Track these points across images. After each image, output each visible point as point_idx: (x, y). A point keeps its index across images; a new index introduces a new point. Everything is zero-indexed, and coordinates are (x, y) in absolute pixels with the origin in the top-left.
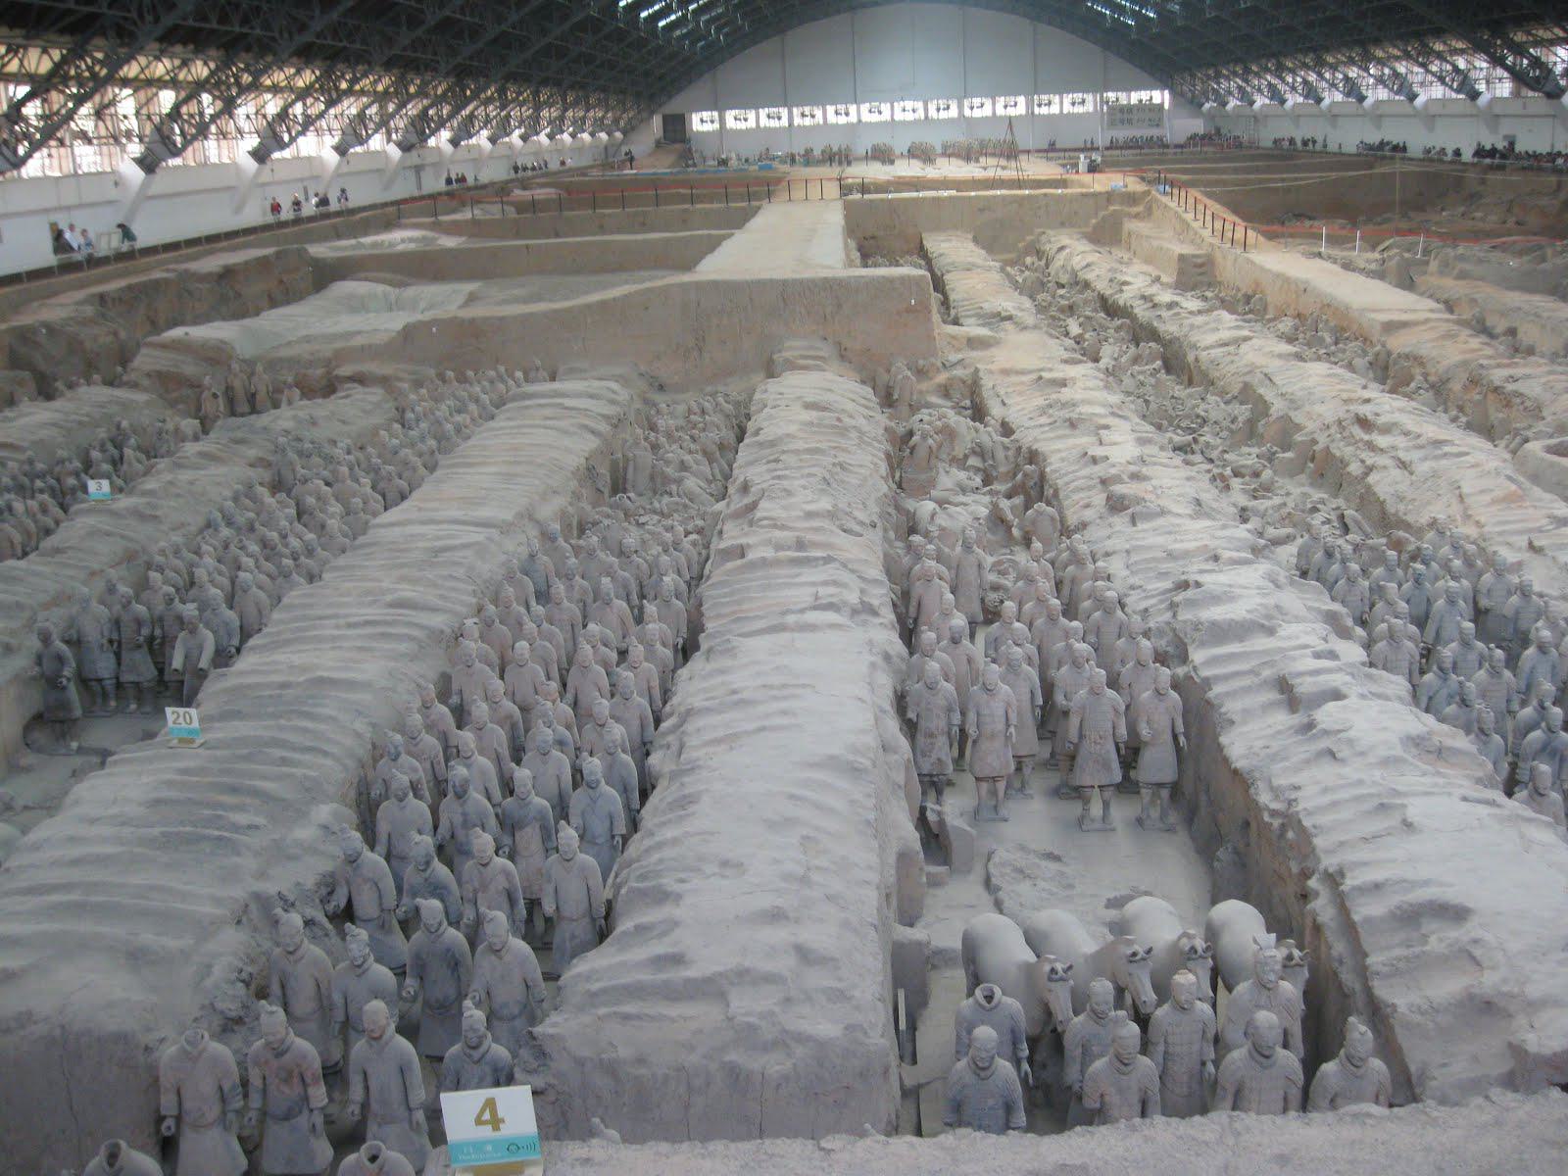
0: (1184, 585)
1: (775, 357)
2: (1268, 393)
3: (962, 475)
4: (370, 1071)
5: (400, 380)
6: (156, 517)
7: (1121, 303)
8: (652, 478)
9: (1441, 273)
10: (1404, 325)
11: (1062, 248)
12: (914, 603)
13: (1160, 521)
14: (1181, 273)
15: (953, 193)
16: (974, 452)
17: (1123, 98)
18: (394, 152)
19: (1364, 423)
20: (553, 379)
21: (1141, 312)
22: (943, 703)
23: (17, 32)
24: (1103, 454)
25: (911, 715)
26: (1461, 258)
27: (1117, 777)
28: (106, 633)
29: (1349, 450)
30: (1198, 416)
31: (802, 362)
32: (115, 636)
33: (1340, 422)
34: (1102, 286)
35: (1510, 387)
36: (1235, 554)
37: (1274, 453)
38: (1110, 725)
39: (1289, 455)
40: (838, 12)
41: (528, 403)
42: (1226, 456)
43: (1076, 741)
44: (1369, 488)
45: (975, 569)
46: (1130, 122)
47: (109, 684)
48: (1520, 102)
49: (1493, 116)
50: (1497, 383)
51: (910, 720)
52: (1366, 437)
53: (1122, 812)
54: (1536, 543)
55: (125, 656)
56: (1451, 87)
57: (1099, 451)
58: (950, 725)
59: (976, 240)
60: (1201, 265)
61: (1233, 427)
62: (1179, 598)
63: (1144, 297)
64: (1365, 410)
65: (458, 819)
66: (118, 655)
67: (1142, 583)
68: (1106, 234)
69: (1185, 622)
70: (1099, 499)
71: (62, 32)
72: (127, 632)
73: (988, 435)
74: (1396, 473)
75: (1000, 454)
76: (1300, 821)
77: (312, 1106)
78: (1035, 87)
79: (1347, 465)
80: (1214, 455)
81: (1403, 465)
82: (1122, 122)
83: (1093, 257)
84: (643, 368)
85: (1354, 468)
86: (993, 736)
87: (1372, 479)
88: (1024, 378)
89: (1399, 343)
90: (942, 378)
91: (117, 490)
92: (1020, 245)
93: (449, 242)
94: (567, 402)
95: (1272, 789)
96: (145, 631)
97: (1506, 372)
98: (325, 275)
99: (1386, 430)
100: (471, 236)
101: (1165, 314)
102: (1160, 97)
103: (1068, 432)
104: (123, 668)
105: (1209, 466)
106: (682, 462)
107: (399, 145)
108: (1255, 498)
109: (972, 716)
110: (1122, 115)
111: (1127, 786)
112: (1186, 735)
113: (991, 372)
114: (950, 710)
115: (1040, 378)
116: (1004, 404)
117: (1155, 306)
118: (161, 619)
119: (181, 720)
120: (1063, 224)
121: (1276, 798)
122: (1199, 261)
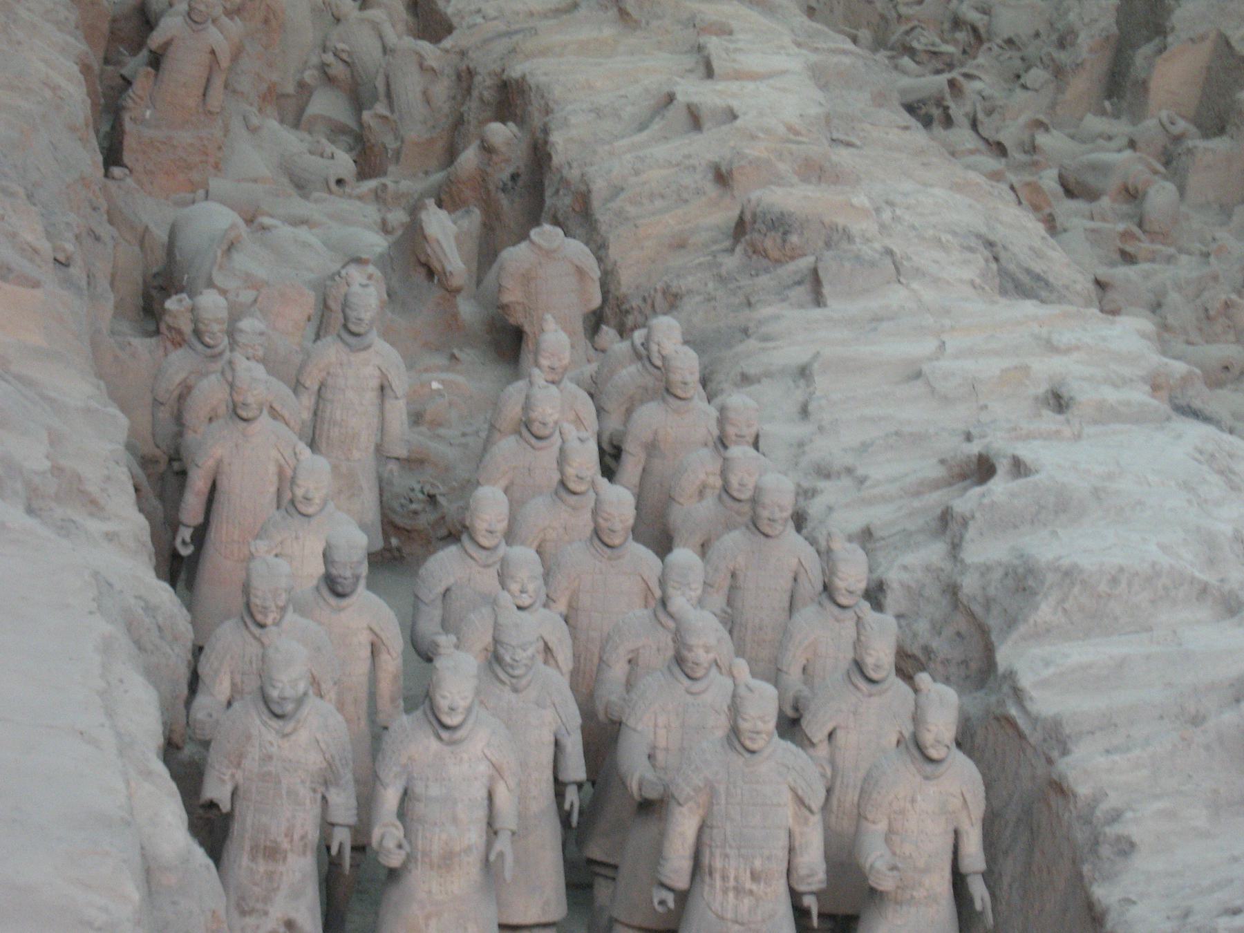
3: (293, 142)
12: (198, 483)
13: (896, 297)
16: (329, 79)
22: (314, 761)
24: (720, 102)
25: (216, 790)
30: (957, 23)
36: (1111, 395)
37: (1178, 139)
38: (783, 842)
39: (1220, 144)
42: (1042, 139)
43: (682, 883)
45: (371, 396)
51: (212, 805)
57: (692, 90)
58: (327, 826)
61: (1062, 57)
62: (968, 500)
67: (849, 460)
69: (985, 570)
75: (410, 86)
80: (1008, 136)
86: (448, 860)
103: (608, 32)
105: (993, 163)
108: (1128, 258)
109: (390, 798)
112: (990, 877)
114: (327, 779)
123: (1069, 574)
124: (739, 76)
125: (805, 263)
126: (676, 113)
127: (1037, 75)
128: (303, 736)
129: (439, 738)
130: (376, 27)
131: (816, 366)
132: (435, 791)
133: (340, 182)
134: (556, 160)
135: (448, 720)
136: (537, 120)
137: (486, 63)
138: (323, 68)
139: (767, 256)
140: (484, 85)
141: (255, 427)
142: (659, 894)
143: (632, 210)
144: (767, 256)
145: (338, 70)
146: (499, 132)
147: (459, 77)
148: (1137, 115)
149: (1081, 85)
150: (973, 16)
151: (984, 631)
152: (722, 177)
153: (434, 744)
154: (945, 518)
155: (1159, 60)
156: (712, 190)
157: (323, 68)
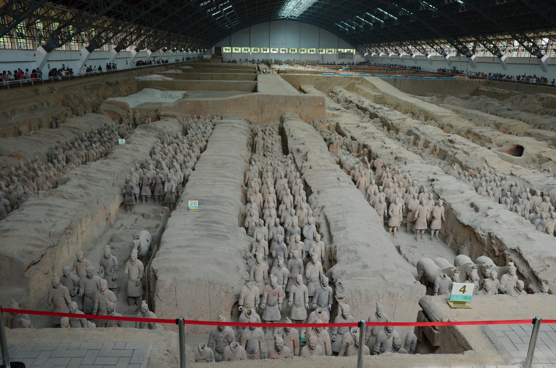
0: (433, 180)
3: (343, 151)
4: (296, 293)
5: (178, 117)
6: (138, 150)
7: (364, 107)
8: (263, 147)
9: (448, 104)
10: (445, 116)
11: (340, 91)
12: (358, 182)
14: (375, 99)
15: (309, 74)
17: (342, 50)
18: (149, 52)
19: (451, 141)
20: (222, 119)
21: (370, 109)
22: (384, 207)
23: (65, 6)
26: (453, 99)
27: (426, 228)
28: (138, 181)
29: (447, 148)
30: (397, 138)
32: (141, 182)
33: (443, 141)
34: (356, 102)
35: (481, 134)
40: (266, 21)
41: (223, 125)
44: (456, 158)
46: (344, 57)
47: (137, 196)
48: (458, 58)
49: (450, 61)
50: (477, 133)
52: (452, 145)
53: (425, 237)
54: (514, 173)
55: (144, 188)
56: (439, 53)
58: (385, 213)
59: (315, 87)
60: (380, 98)
62: (433, 183)
63: (371, 106)
64: (450, 138)
65: (275, 232)
66: (141, 188)
68: (351, 88)
69: (437, 189)
70: (392, 157)
71: (76, 8)
72: (145, 181)
73: (348, 140)
74: (465, 155)
75: (354, 145)
76: (496, 237)
77: (279, 302)
78: (319, 46)
79: (447, 152)
81: (465, 153)
82: (342, 57)
83: (351, 94)
84: (246, 118)
85: (450, 153)
87: (457, 156)
88: (353, 126)
89: (445, 121)
90: (327, 124)
91: (127, 143)
92: (327, 90)
93: (167, 79)
94: (235, 125)
95: (481, 229)
96: (150, 181)
97: (480, 130)
98: (142, 86)
99: (459, 143)
100: (175, 78)
101: (379, 111)
102: (353, 51)
104: (142, 191)
106: (272, 143)
107: (151, 50)
110: (342, 55)
111: (428, 231)
113: (342, 123)
115: (359, 126)
116: (349, 132)
117: (374, 108)
118: (155, 178)
119: (193, 204)
120: (339, 85)
121: (484, 232)
122: (380, 97)
123: (446, 190)
125: (404, 161)
126: (384, 148)
127: (406, 143)
137: (362, 143)
138: (344, 144)
140: (362, 145)
142: (414, 219)
145: (345, 144)
146: (365, 149)
148: (417, 146)
149: (411, 144)
151: (438, 195)
152: (392, 153)
154: (431, 185)
157: (344, 144)
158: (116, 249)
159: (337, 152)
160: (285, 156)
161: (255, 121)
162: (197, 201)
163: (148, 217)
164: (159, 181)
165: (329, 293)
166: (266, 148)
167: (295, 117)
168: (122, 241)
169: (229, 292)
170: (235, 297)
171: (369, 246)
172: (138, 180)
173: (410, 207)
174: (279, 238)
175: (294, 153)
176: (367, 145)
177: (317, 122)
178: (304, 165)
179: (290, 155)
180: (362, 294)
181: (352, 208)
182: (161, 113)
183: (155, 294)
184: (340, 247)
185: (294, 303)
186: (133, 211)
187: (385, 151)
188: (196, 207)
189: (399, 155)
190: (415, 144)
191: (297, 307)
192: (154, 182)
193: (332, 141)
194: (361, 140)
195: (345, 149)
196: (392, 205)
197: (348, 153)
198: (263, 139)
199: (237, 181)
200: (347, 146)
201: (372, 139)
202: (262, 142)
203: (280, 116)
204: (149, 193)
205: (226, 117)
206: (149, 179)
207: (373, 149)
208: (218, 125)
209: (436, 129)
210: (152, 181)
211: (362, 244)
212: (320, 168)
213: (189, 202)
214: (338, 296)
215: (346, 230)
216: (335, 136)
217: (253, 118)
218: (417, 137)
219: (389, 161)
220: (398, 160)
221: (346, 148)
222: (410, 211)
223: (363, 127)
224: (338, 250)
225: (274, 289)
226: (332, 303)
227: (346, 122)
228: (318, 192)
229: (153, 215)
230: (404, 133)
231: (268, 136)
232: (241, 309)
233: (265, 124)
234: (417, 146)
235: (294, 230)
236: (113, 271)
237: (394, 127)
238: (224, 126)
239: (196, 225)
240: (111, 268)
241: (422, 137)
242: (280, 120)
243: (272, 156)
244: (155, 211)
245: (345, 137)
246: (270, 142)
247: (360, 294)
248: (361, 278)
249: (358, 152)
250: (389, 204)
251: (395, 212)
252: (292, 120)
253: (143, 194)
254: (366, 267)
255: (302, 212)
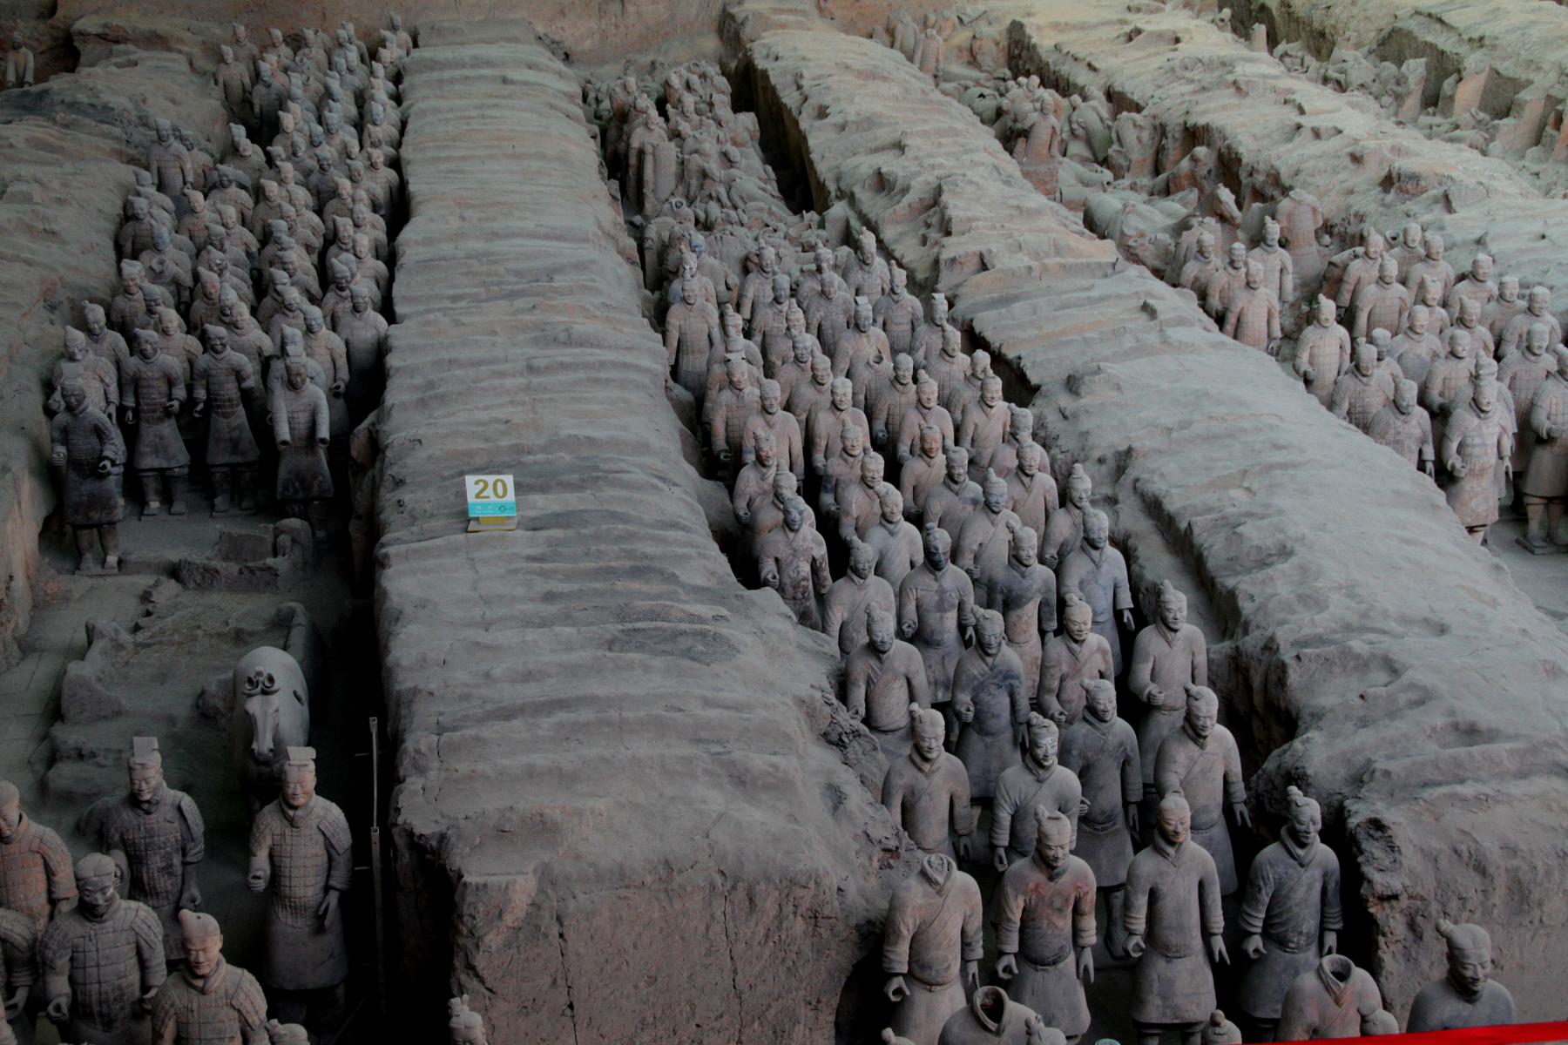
1: (734, 10)
2: (1444, 42)
4: (1164, 889)
6: (53, 233)
8: (681, 177)
22: (1417, 432)
28: (114, 397)
31: (783, 18)
32: (130, 402)
41: (447, 74)
45: (1277, 274)
55: (149, 433)
61: (1399, 89)
66: (131, 436)
73: (1094, 112)
75: (1130, 136)
84: (540, 29)
86: (1483, 471)
90: (963, 37)
103: (1234, 101)
109: (1454, 446)
113: (1039, 28)
115: (1138, 32)
116: (1089, 65)
119: (489, 492)
124: (1318, 113)
126: (1306, 134)
128: (1414, 422)
129: (1479, 417)
130: (1094, 109)
131: (1488, 239)
132: (1477, 441)
133: (1108, 183)
134: (1245, 161)
135: (1485, 408)
136: (1219, 143)
137: (1174, 120)
138: (1072, 131)
139: (1408, 192)
140: (1174, 131)
141: (1256, 292)
143: (1309, 179)
144: (1408, 192)
145: (1080, 132)
146: (1201, 151)
147: (1155, 128)
148: (1447, 113)
149: (1413, 102)
150: (1335, 75)
152: (1356, 159)
153: (1477, 421)
155: (1460, 85)
156: (1351, 166)
157: (1072, 131)
158: (100, 759)
159: (1053, 175)
160: (811, 216)
161: (588, 44)
162: (509, 479)
163: (208, 578)
164: (230, 390)
165: (1325, 875)
166: (694, 183)
167: (790, 11)
168: (118, 714)
169: (827, 911)
170: (855, 937)
171: (1442, 630)
172: (113, 388)
173: (1542, 421)
174: (987, 625)
175: (864, 196)
176: (1207, 128)
177: (908, 30)
178: (945, 256)
179: (838, 210)
180: (1491, 870)
181: (1278, 447)
182: (79, 25)
183: (458, 963)
184: (1297, 644)
185: (1151, 935)
186: (112, 559)
187: (1311, 148)
188: (502, 508)
189: (1404, 164)
190: (1433, 100)
191: (1169, 959)
192: (201, 394)
193: (1027, 125)
194: (1167, 103)
195: (1084, 161)
196: (1463, 418)
197: (1108, 175)
198: (675, 135)
199: (646, 362)
200: (1089, 142)
201: (1227, 97)
202: (670, 150)
203: (715, 12)
204: (178, 457)
205: (437, 31)
206: (171, 383)
207: (1247, 148)
208: (424, 77)
209: (1540, 9)
210: (190, 389)
211: (1404, 620)
212: (1034, 264)
213: (470, 480)
214: (1379, 889)
215: (1294, 560)
216: (1026, 96)
217: (578, 31)
218: (1444, 68)
219: (1351, 200)
220: (1401, 190)
221: (1086, 153)
222: (1547, 440)
223: (1159, 36)
224: (1287, 655)
225: (1059, 875)
226: (1339, 926)
227: (1062, 19)
228: (1072, 384)
229: (234, 568)
230: (1365, 49)
231: (696, 118)
232: (898, 991)
233: (645, 60)
234: (1447, 113)
235: (1026, 583)
236: (178, 869)
237: (1297, 20)
238: (452, 81)
239: (549, 597)
240: (168, 856)
241: (1473, 61)
242: (720, 31)
243: (745, 219)
244: (233, 548)
245: (1076, 98)
246: (710, 147)
247: (1482, 870)
248: (1467, 790)
249: (1157, 171)
250: (1441, 416)
251: (1476, 451)
252: (783, 26)
253: (149, 461)
254: (1471, 733)
255: (1028, 489)
